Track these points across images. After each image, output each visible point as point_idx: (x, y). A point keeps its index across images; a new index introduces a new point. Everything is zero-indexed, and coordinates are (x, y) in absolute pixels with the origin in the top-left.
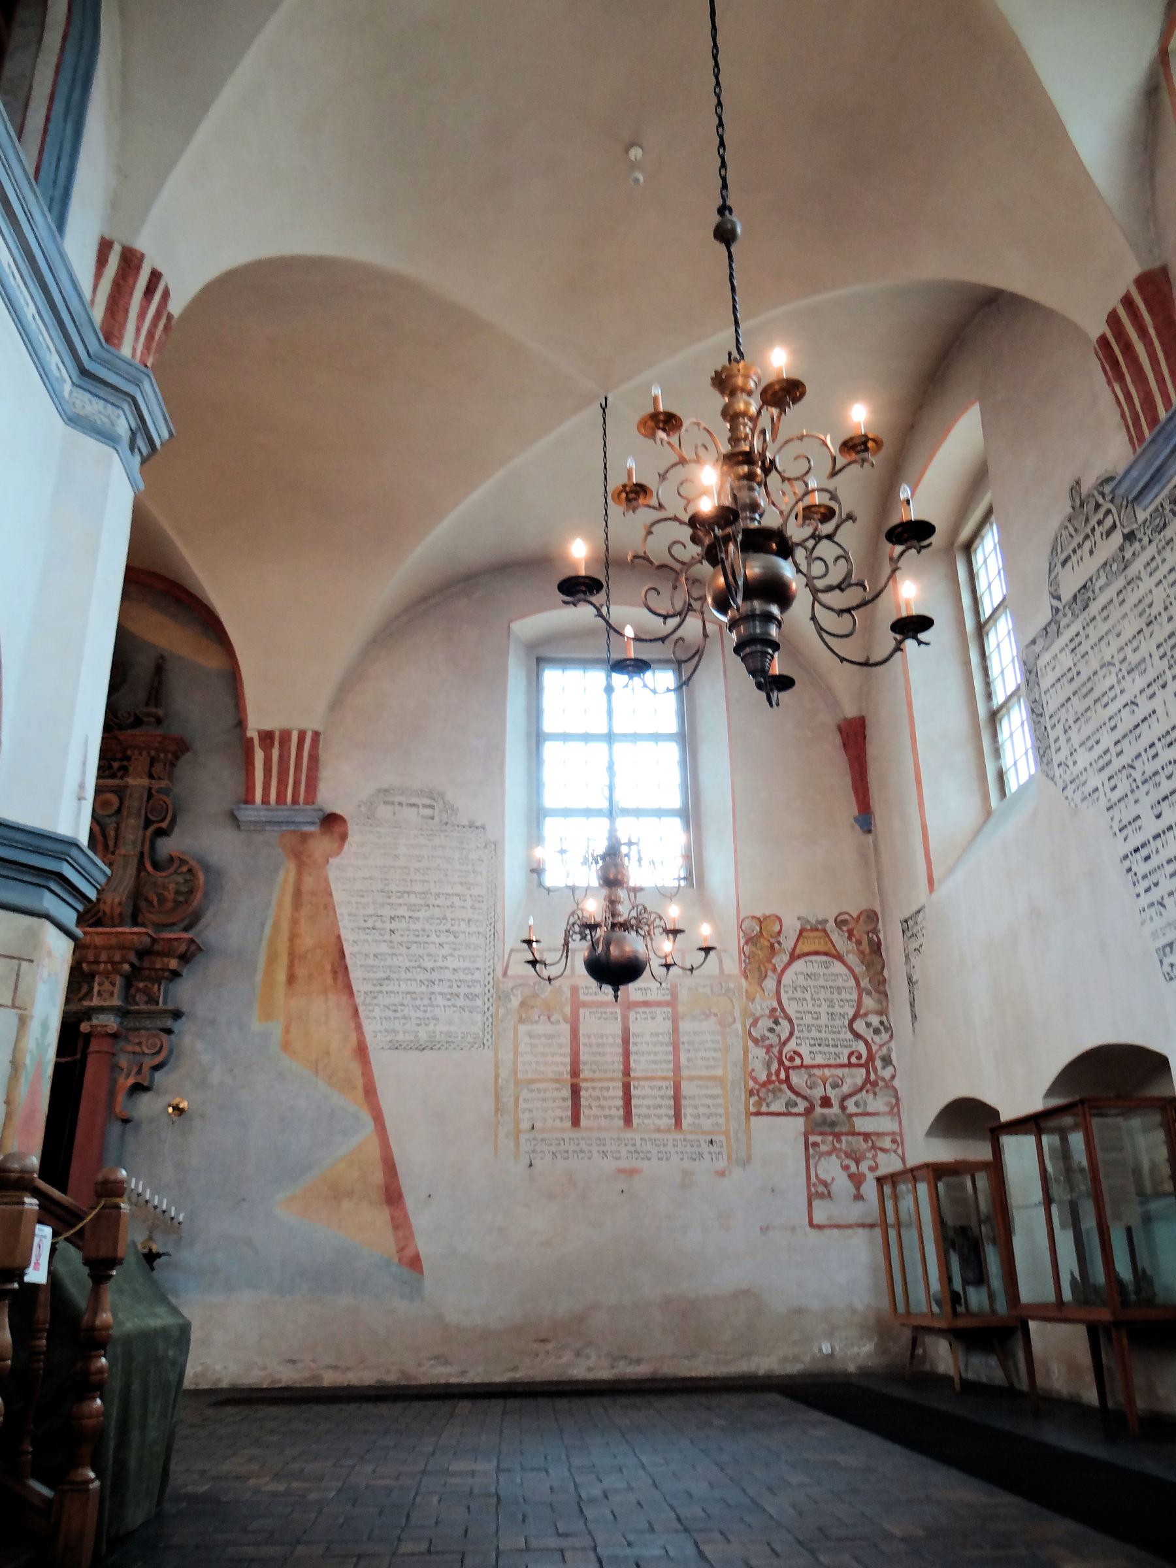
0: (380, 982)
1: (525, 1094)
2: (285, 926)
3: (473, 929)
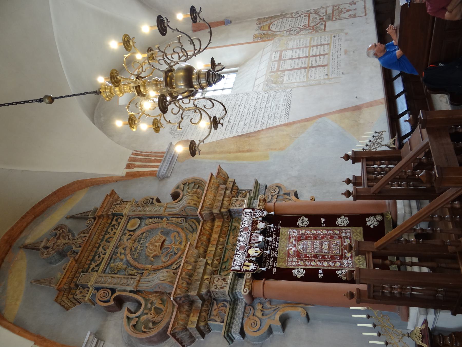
2: (222, 156)
3: (240, 100)
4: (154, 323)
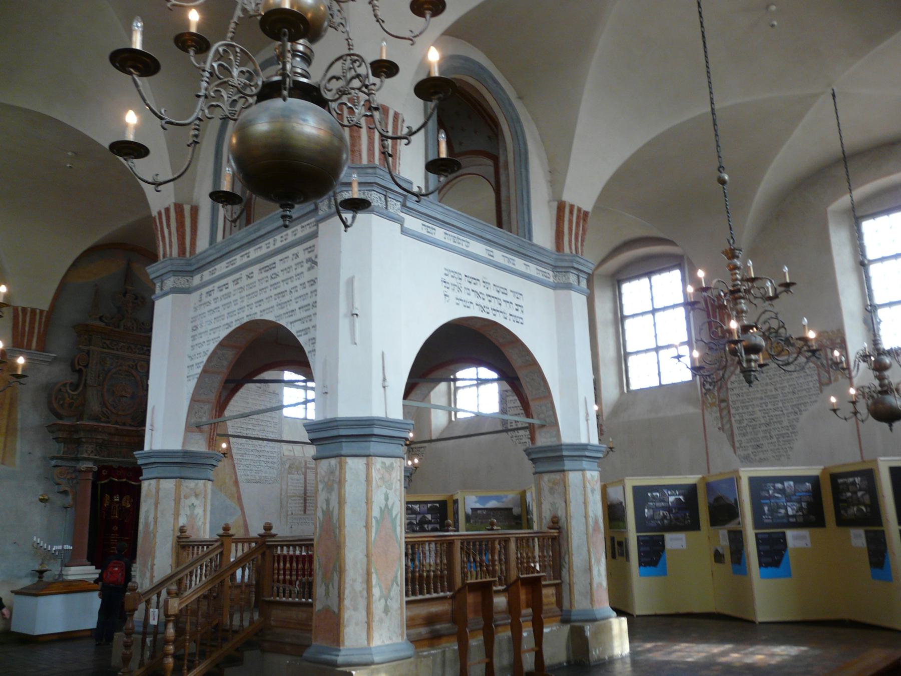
0: (242, 455)
1: (290, 501)
4: (62, 405)
